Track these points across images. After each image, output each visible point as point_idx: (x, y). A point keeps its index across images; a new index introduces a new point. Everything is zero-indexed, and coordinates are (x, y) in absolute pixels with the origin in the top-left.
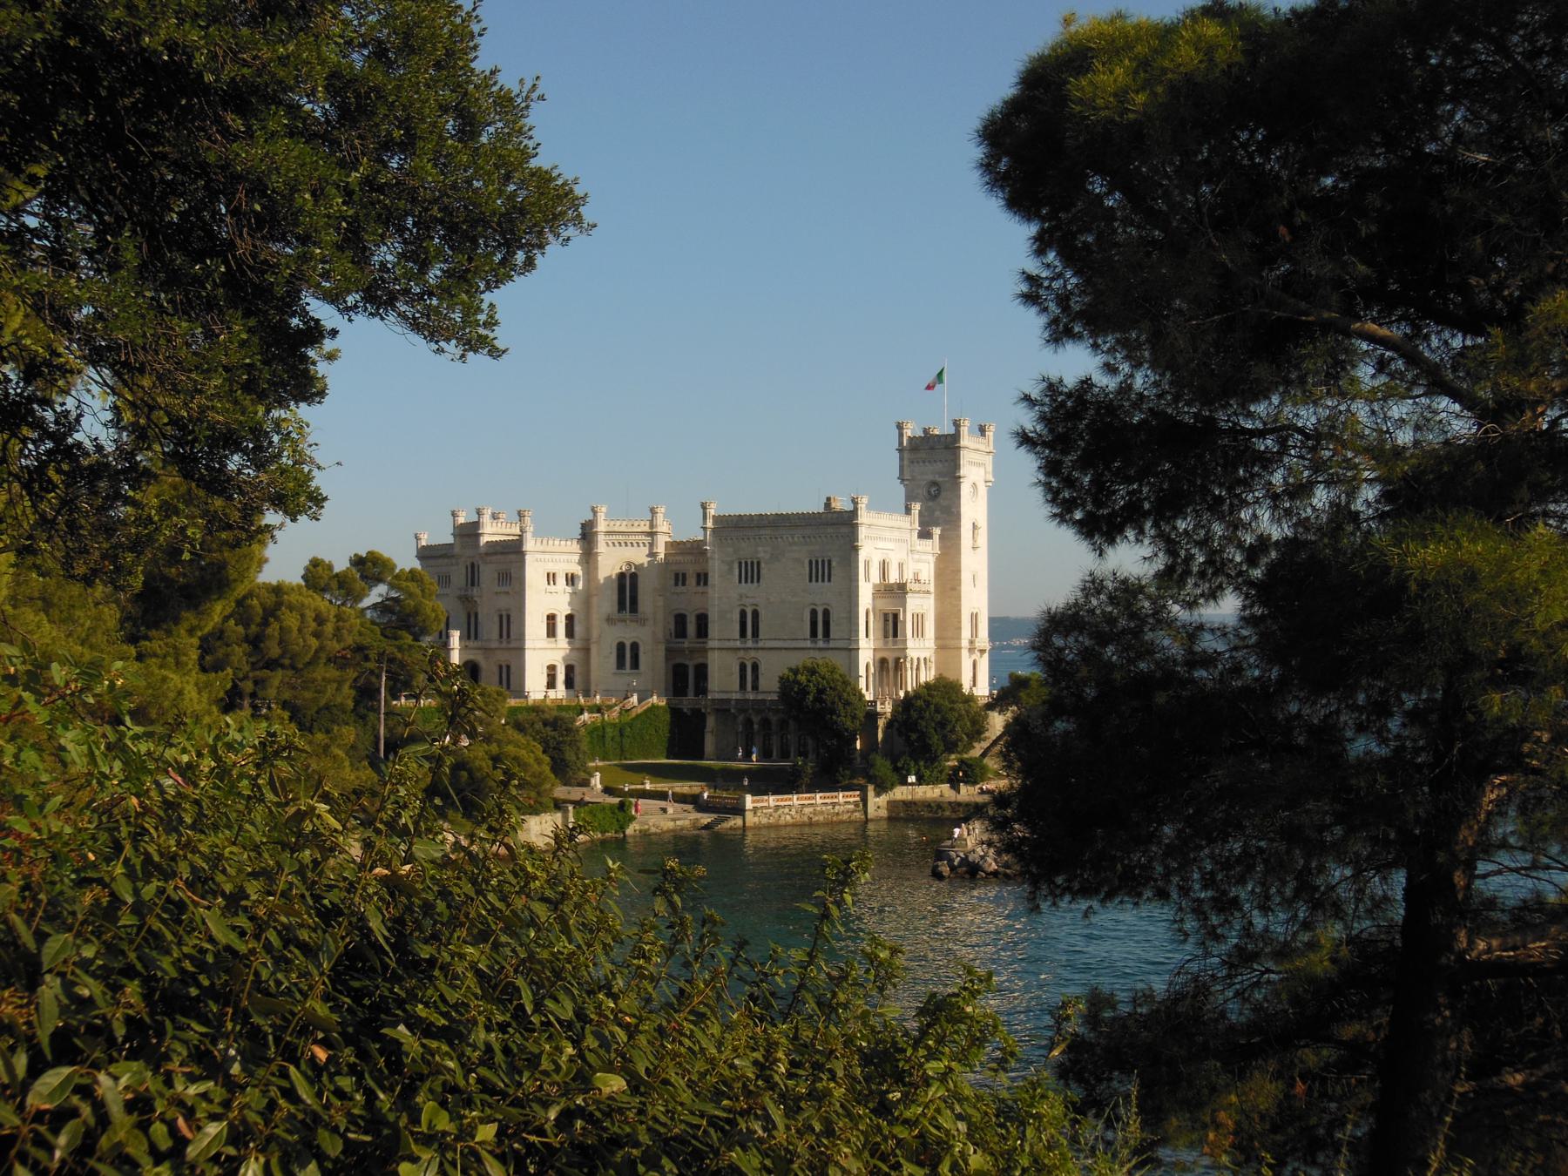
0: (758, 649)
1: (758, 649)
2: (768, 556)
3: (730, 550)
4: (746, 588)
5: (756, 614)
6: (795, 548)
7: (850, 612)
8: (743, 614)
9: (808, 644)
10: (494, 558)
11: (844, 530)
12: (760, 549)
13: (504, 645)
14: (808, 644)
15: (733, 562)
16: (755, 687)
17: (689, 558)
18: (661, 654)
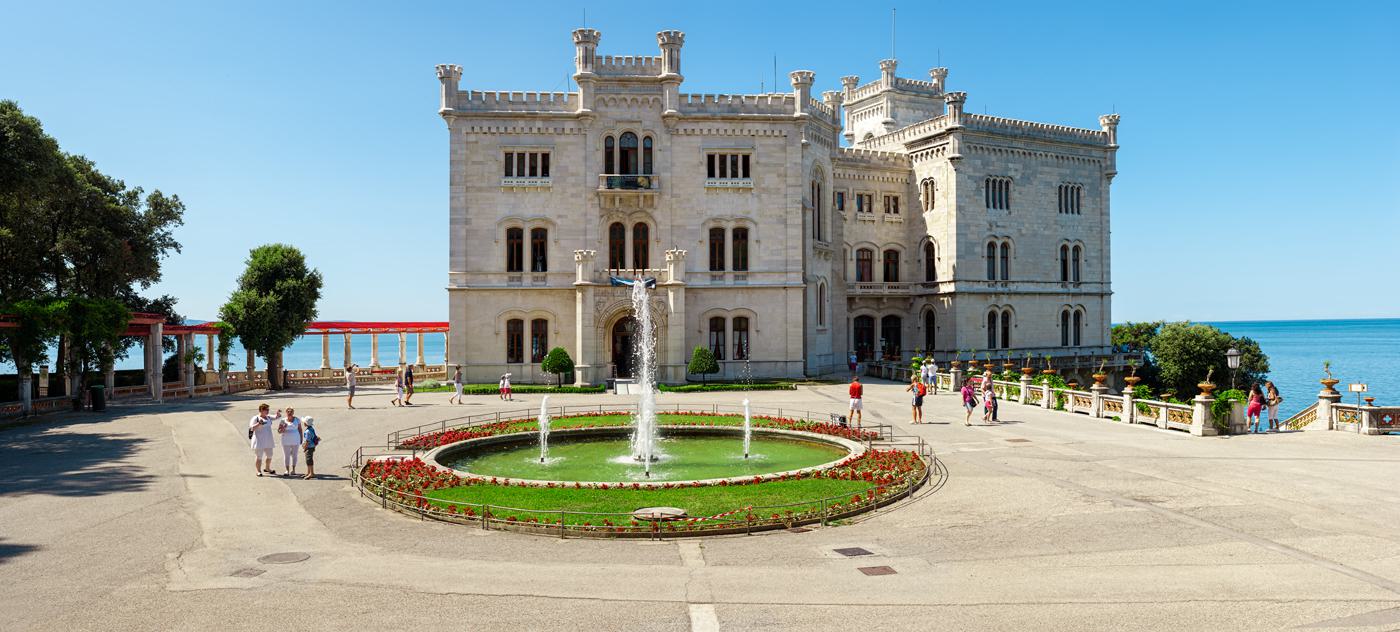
0: (1009, 294)
1: (1009, 294)
2: (1018, 177)
3: (978, 162)
4: (995, 214)
5: (1005, 246)
6: (1046, 169)
7: (1101, 250)
8: (992, 246)
9: (1058, 288)
10: (705, 126)
11: (1096, 153)
12: (1011, 165)
13: (729, 280)
14: (1058, 288)
15: (981, 179)
16: (1005, 343)
17: (852, 172)
18: (846, 301)
